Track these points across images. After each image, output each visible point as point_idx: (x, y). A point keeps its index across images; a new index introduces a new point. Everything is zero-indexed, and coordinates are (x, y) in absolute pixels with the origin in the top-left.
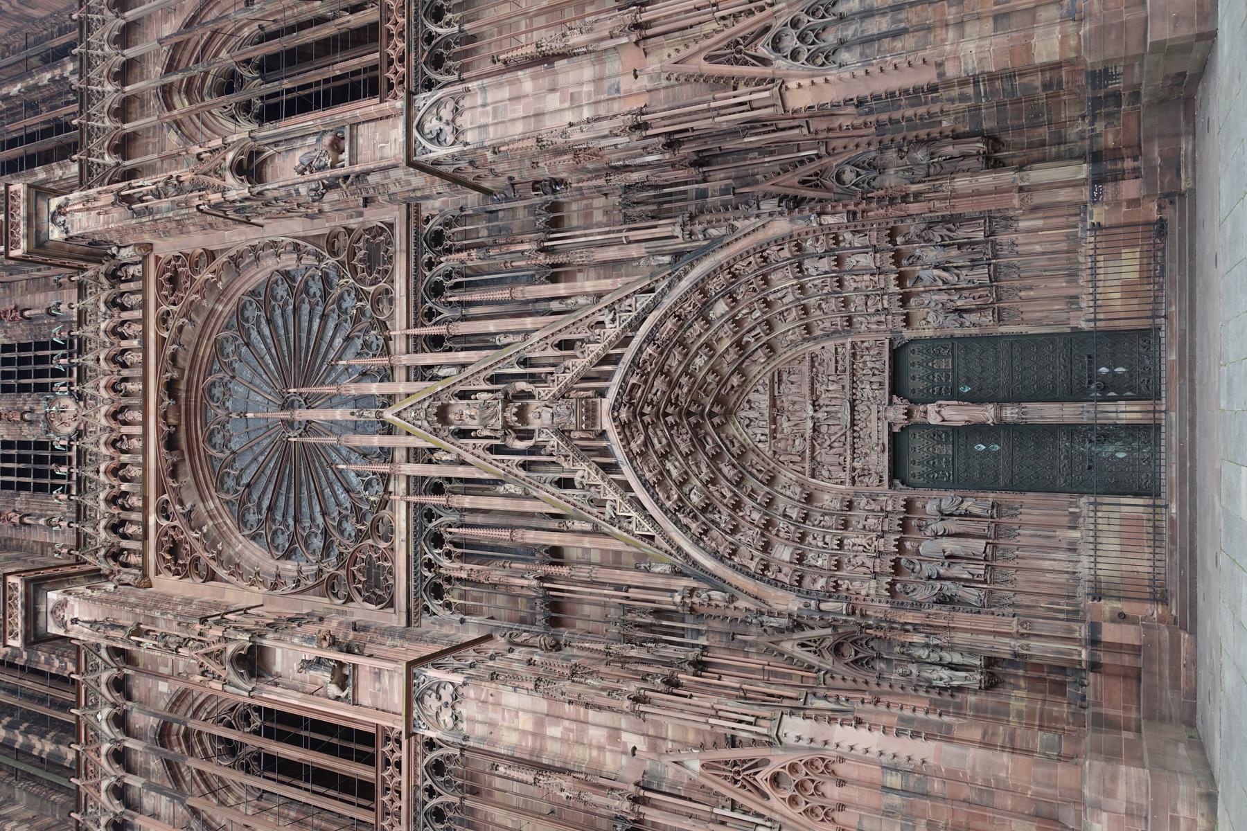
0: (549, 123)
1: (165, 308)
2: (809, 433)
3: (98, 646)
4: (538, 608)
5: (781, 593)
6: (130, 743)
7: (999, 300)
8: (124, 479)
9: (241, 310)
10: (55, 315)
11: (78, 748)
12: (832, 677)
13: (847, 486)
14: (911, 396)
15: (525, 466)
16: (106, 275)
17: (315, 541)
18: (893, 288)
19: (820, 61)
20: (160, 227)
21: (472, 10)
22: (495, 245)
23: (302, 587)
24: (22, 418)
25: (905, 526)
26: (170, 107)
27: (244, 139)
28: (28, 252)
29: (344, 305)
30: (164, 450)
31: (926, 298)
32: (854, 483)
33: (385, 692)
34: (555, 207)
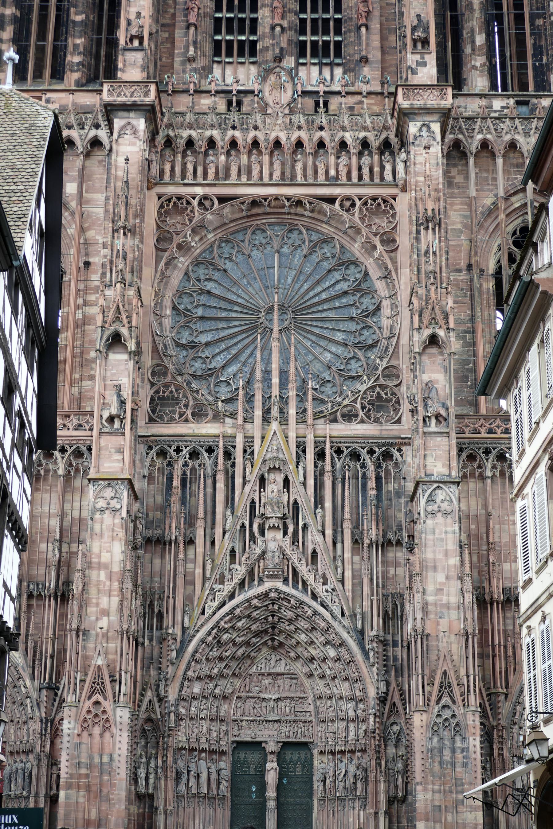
0: (429, 575)
1: (358, 203)
2: (262, 695)
4: (156, 532)
5: (177, 690)
7: (329, 800)
8: (228, 154)
9: (356, 263)
13: (233, 718)
15: (243, 526)
16: (387, 138)
18: (338, 748)
19: (436, 728)
22: (377, 507)
23: (157, 338)
24: (276, 25)
25: (212, 752)
28: (400, 109)
29: (353, 362)
30: (251, 199)
31: (332, 764)
32: (234, 721)
33: (110, 456)
34: (399, 543)
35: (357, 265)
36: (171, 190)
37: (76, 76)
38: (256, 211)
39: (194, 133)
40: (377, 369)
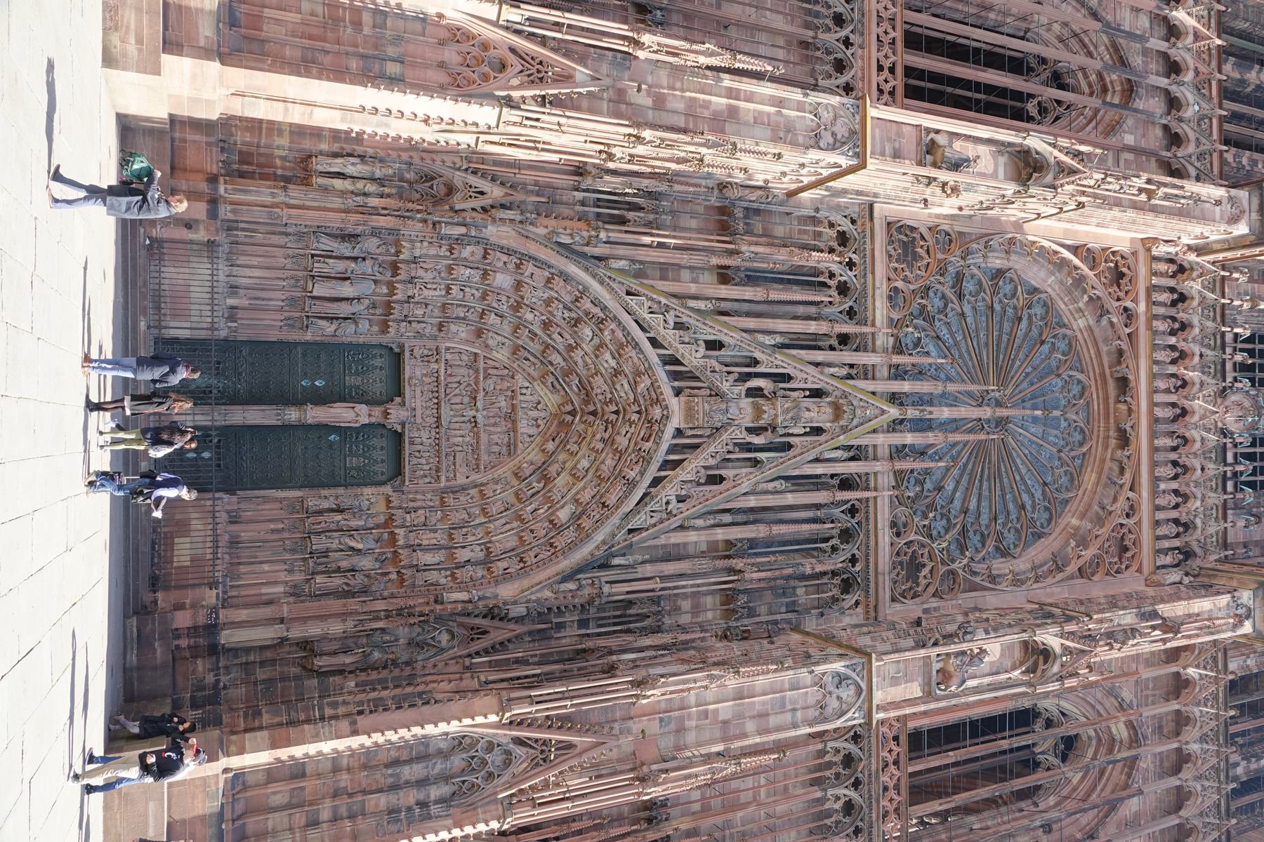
1: (1131, 521)
2: (480, 396)
3: (1198, 179)
5: (504, 242)
6: (1163, 82)
7: (301, 520)
8: (1173, 348)
10: (1252, 515)
11: (1218, 76)
12: (454, 163)
13: (443, 346)
14: (384, 432)
15: (756, 362)
16: (1195, 555)
17: (971, 288)
18: (400, 532)
20: (1134, 602)
21: (813, 810)
22: (789, 578)
23: (983, 241)
25: (388, 307)
26: (1130, 725)
27: (1041, 684)
29: (944, 522)
30: (1131, 377)
33: (889, 140)
34: (729, 613)
35: (1049, 521)
36: (1142, 270)
37: (1230, 159)
38: (1111, 385)
39: (1195, 303)
40: (953, 561)
